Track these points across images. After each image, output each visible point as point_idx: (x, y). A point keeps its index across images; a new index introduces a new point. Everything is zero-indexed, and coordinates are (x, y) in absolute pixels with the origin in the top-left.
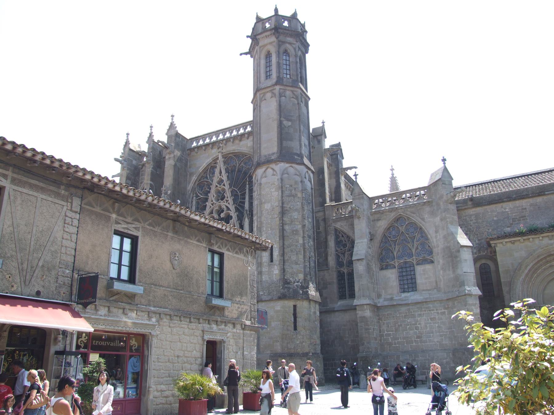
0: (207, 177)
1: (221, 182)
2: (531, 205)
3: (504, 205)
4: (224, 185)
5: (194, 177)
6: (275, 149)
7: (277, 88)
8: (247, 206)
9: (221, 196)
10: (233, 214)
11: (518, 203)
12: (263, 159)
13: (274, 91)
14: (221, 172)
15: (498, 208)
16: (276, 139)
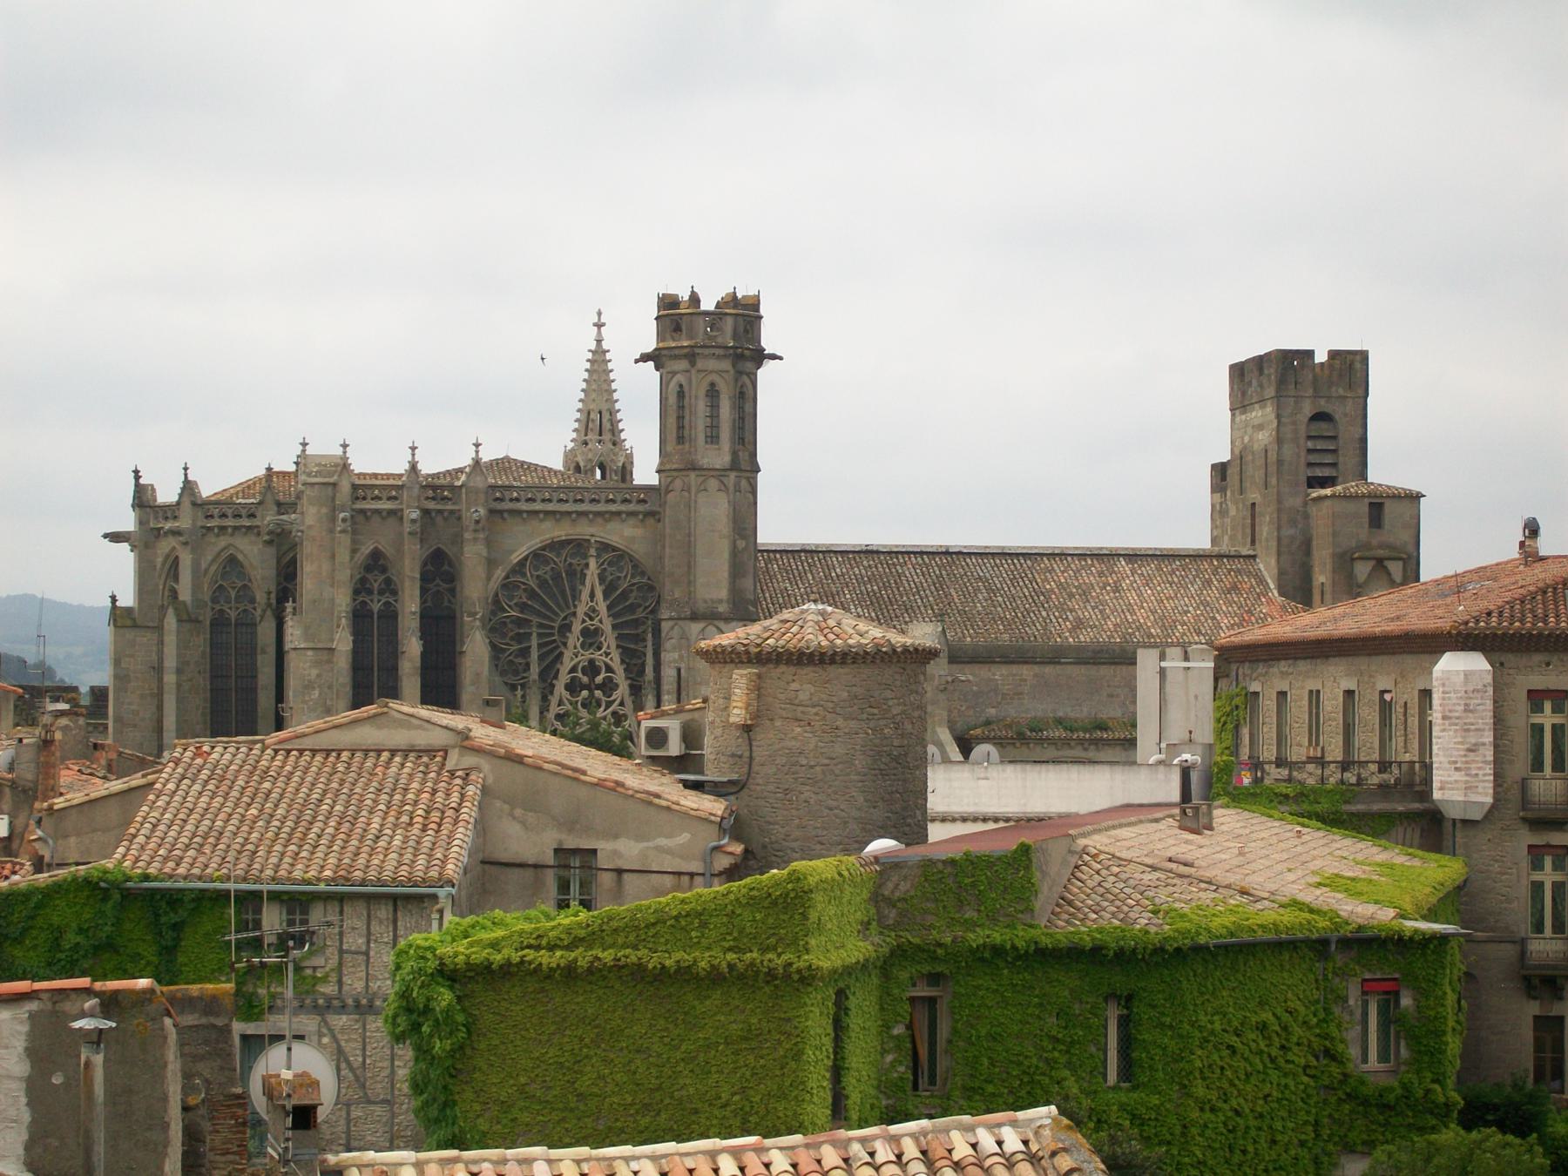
0: (524, 575)
1: (592, 613)
2: (1035, 675)
3: (994, 668)
4: (601, 621)
5: (499, 572)
6: (723, 593)
7: (733, 475)
8: (649, 670)
9: (591, 637)
10: (620, 676)
11: (1015, 669)
12: (701, 607)
13: (725, 480)
14: (592, 596)
15: (984, 672)
16: (726, 575)
